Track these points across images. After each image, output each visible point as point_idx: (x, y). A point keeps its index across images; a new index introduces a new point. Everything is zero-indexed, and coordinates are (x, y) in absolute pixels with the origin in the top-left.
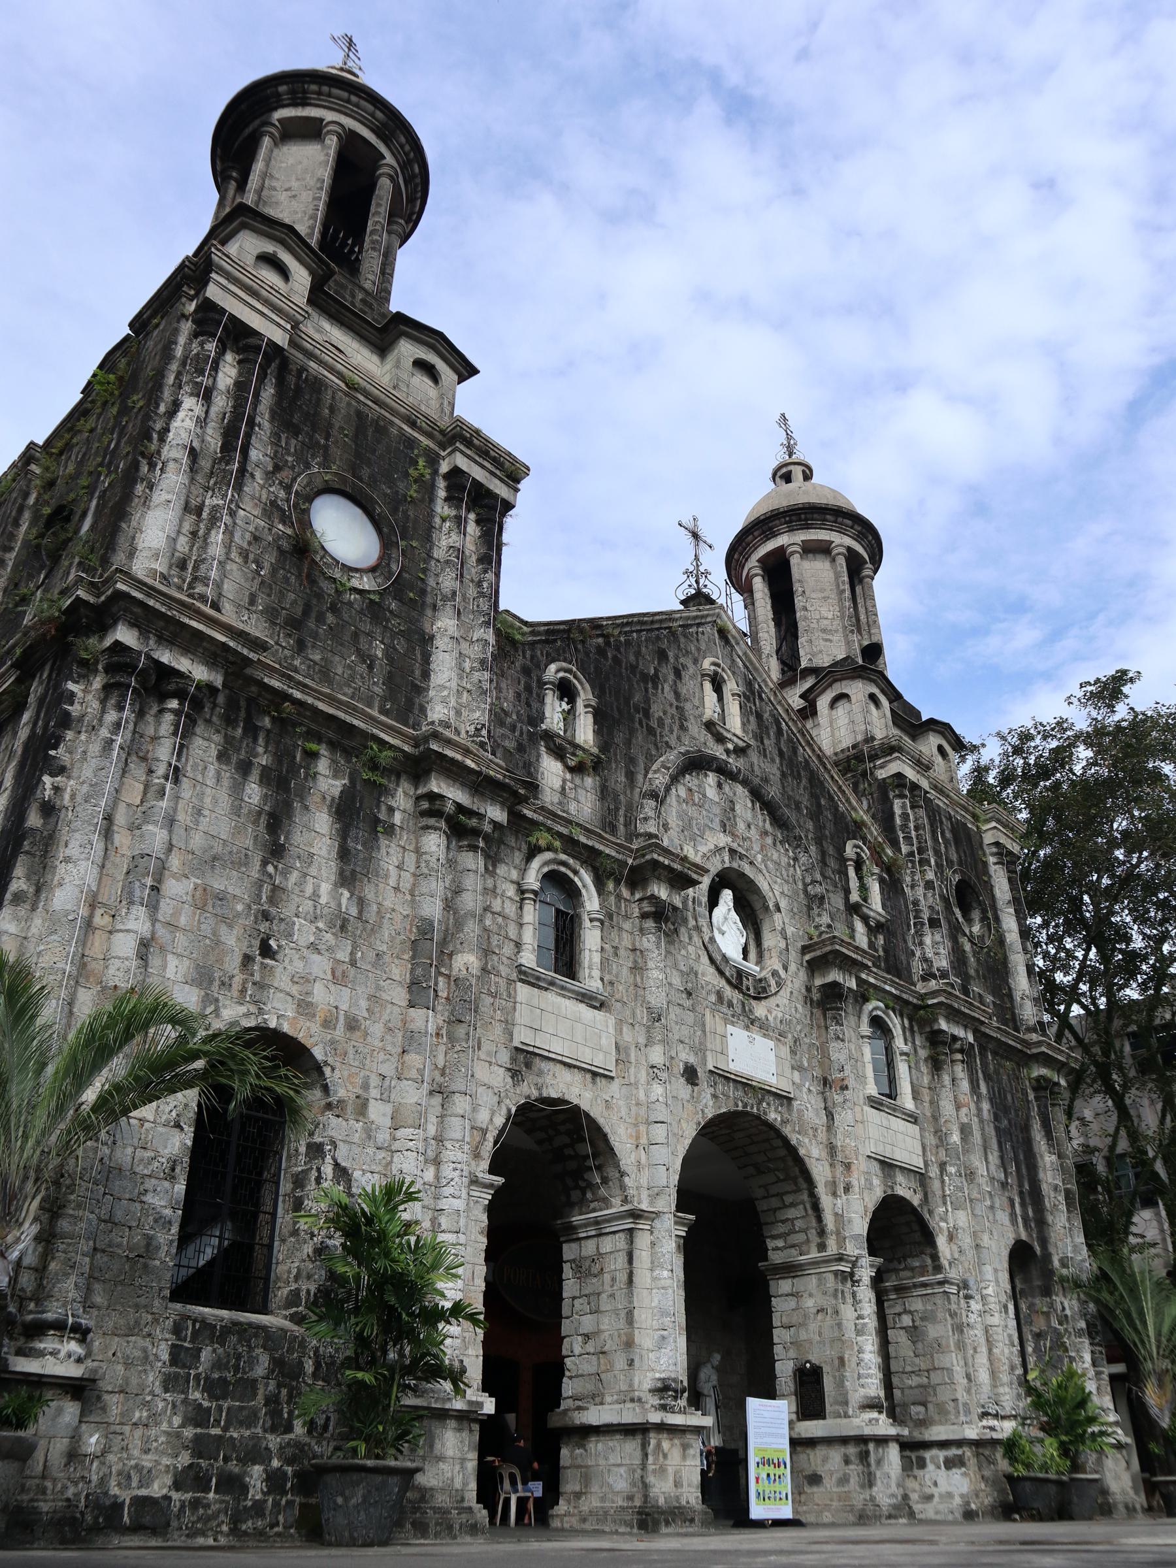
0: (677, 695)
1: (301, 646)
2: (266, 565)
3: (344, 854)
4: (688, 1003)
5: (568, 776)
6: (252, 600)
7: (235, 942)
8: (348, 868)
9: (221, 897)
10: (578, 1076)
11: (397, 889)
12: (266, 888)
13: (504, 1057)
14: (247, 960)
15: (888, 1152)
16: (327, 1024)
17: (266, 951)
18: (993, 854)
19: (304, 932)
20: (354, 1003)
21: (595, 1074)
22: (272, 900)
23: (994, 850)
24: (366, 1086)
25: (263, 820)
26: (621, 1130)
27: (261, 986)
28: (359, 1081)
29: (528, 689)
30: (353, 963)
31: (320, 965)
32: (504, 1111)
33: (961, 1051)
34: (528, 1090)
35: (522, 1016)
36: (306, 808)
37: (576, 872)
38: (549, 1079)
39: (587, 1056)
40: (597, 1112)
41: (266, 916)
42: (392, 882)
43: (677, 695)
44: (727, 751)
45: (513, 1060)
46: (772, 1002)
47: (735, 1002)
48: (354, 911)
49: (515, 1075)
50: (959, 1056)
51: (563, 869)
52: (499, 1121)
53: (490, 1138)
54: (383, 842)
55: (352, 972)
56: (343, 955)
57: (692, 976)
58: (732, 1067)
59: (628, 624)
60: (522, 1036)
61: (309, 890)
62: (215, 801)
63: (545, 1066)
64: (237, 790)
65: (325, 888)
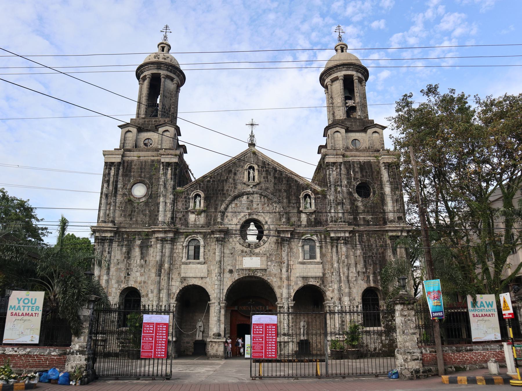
0: (234, 180)
1: (131, 219)
2: (123, 207)
3: (142, 254)
4: (231, 256)
5: (197, 216)
6: (121, 215)
7: (123, 275)
8: (142, 256)
9: (120, 269)
10: (197, 279)
11: (153, 256)
12: (128, 265)
13: (179, 280)
14: (125, 277)
15: (305, 275)
16: (140, 283)
17: (128, 275)
18: (383, 166)
19: (135, 269)
20: (145, 278)
21: (202, 278)
22: (129, 266)
23: (383, 165)
24: (148, 292)
25: (126, 253)
26: (209, 287)
27: (128, 281)
28: (146, 291)
29: (186, 201)
30: (144, 272)
31: (138, 274)
32: (179, 289)
33: (343, 240)
34: (185, 284)
35: (182, 271)
36: (134, 249)
38: (190, 281)
39: (199, 275)
40: (203, 285)
41: (128, 269)
42: (152, 255)
43: (234, 180)
44: (252, 188)
45: (181, 280)
46: (262, 247)
47: (248, 251)
48: (144, 263)
49: (182, 282)
50: (342, 241)
51: (194, 238)
52: (178, 291)
53: (176, 296)
54: (150, 248)
55: (144, 273)
56: (142, 271)
57: (233, 249)
58: (244, 267)
59: (215, 171)
60: (183, 275)
61: (135, 262)
62: (118, 253)
63: (189, 279)
64: (121, 250)
65: (138, 261)
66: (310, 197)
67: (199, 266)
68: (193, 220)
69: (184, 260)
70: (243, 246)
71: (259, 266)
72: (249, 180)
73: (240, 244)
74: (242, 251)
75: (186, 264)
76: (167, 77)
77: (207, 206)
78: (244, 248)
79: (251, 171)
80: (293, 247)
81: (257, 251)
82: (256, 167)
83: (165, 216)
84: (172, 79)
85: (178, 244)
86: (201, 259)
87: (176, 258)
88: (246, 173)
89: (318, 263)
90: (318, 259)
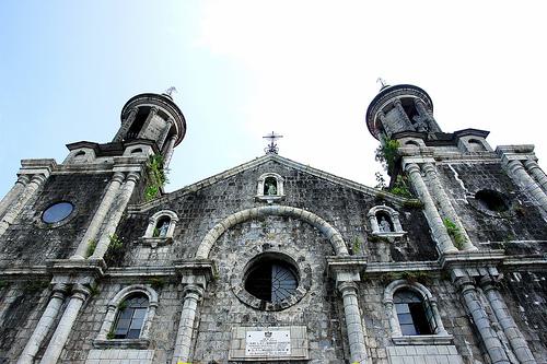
37: (145, 290)
46: (294, 309)
66: (388, 218)
67: (133, 353)
68: (146, 257)
69: (102, 337)
70: (248, 306)
71: (289, 353)
72: (266, 192)
73: (241, 302)
74: (246, 318)
75: (103, 346)
76: (160, 114)
77: (180, 235)
78: (250, 310)
79: (271, 187)
80: (370, 307)
81: (281, 316)
82: (278, 177)
83: (91, 252)
84: (166, 118)
85: (98, 303)
86: (145, 335)
87: (83, 334)
88: (261, 187)
89: (443, 342)
90: (443, 333)
